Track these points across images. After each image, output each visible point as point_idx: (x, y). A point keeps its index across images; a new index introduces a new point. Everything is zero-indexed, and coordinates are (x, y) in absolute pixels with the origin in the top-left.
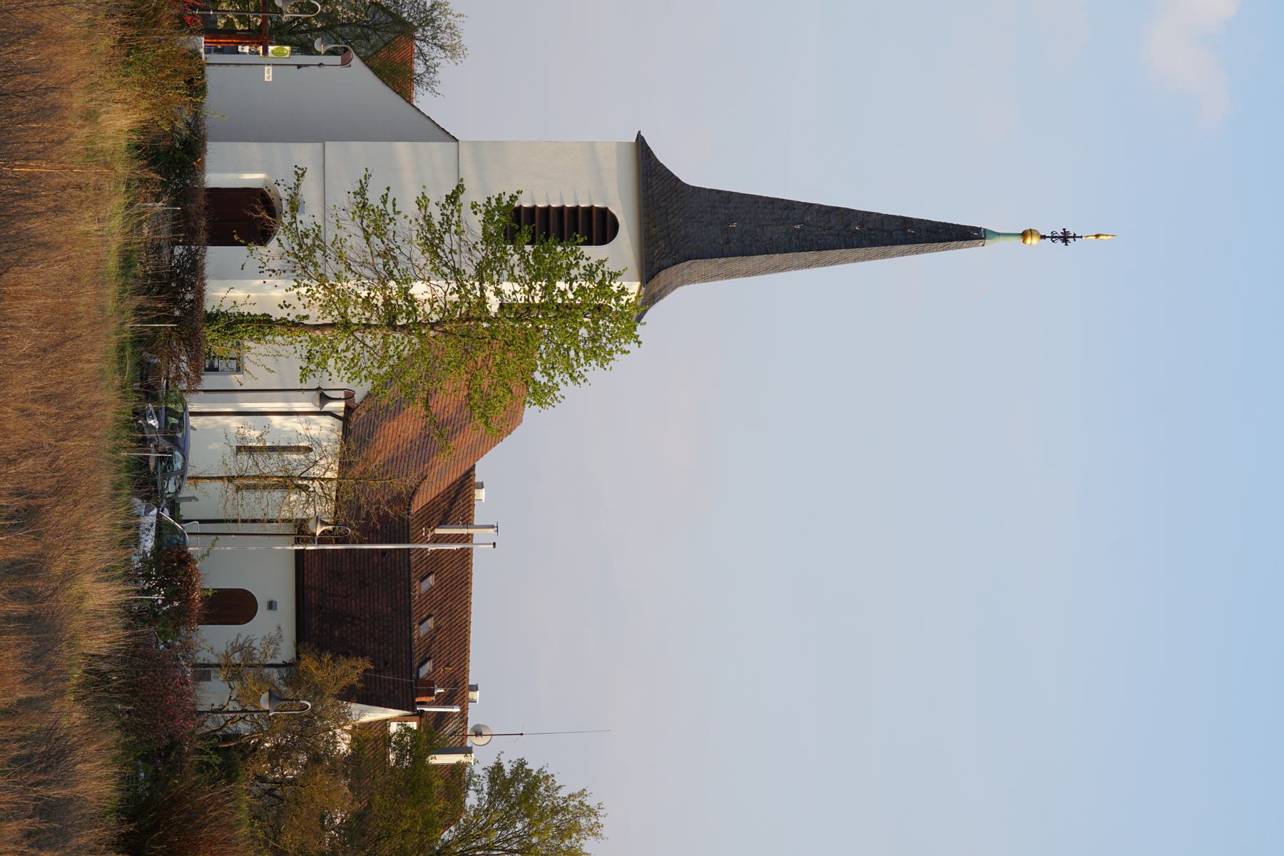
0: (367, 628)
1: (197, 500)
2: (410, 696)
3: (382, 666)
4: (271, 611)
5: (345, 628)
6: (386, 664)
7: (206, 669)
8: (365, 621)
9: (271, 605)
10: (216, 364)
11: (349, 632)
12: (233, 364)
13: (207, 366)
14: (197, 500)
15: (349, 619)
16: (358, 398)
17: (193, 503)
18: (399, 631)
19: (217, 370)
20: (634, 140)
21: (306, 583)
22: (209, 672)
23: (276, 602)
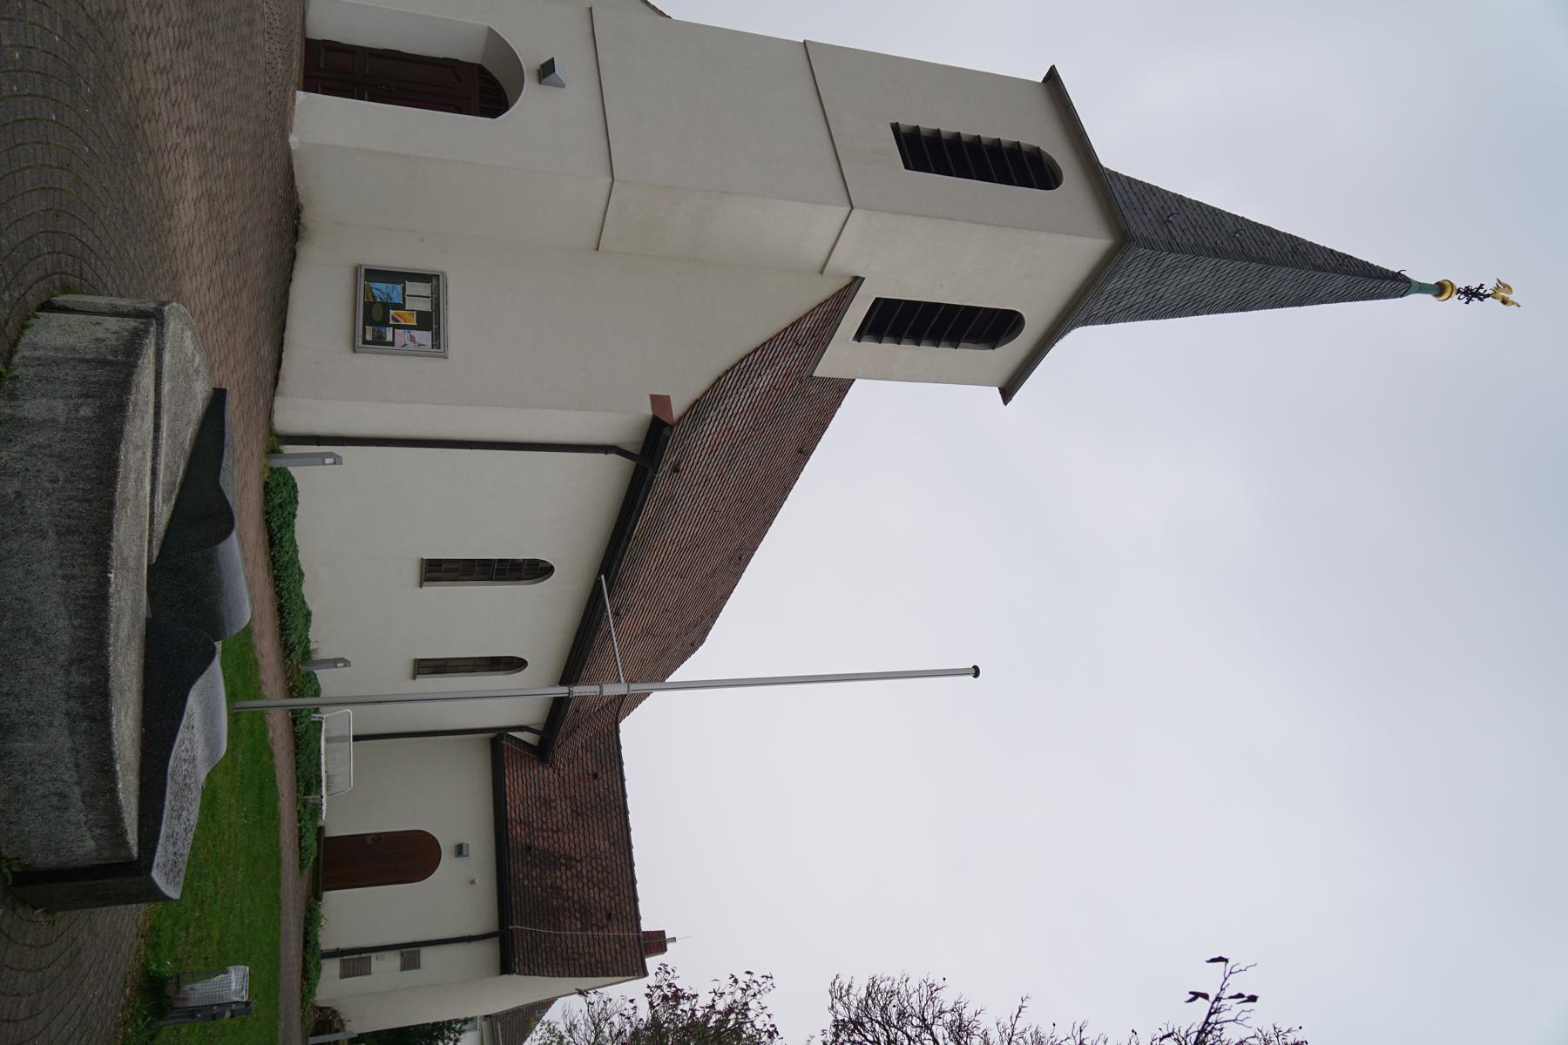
0: (585, 872)
1: (346, 663)
2: (638, 956)
3: (605, 922)
4: (461, 860)
5: (558, 874)
6: (609, 916)
7: (363, 955)
8: (581, 861)
9: (460, 850)
10: (389, 338)
11: (564, 877)
12: (424, 337)
13: (369, 338)
14: (346, 663)
15: (563, 861)
16: (678, 408)
17: (340, 671)
18: (620, 871)
19: (392, 344)
20: (1039, 77)
21: (509, 814)
22: (370, 957)
23: (468, 845)
